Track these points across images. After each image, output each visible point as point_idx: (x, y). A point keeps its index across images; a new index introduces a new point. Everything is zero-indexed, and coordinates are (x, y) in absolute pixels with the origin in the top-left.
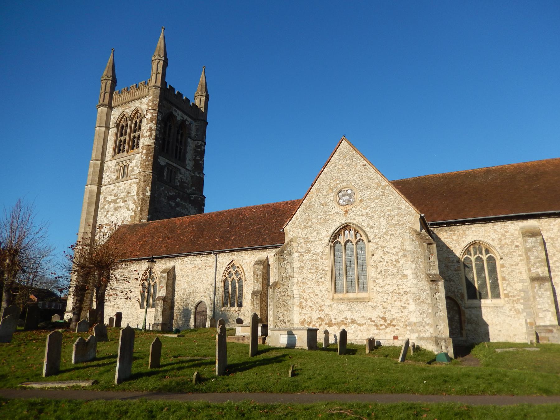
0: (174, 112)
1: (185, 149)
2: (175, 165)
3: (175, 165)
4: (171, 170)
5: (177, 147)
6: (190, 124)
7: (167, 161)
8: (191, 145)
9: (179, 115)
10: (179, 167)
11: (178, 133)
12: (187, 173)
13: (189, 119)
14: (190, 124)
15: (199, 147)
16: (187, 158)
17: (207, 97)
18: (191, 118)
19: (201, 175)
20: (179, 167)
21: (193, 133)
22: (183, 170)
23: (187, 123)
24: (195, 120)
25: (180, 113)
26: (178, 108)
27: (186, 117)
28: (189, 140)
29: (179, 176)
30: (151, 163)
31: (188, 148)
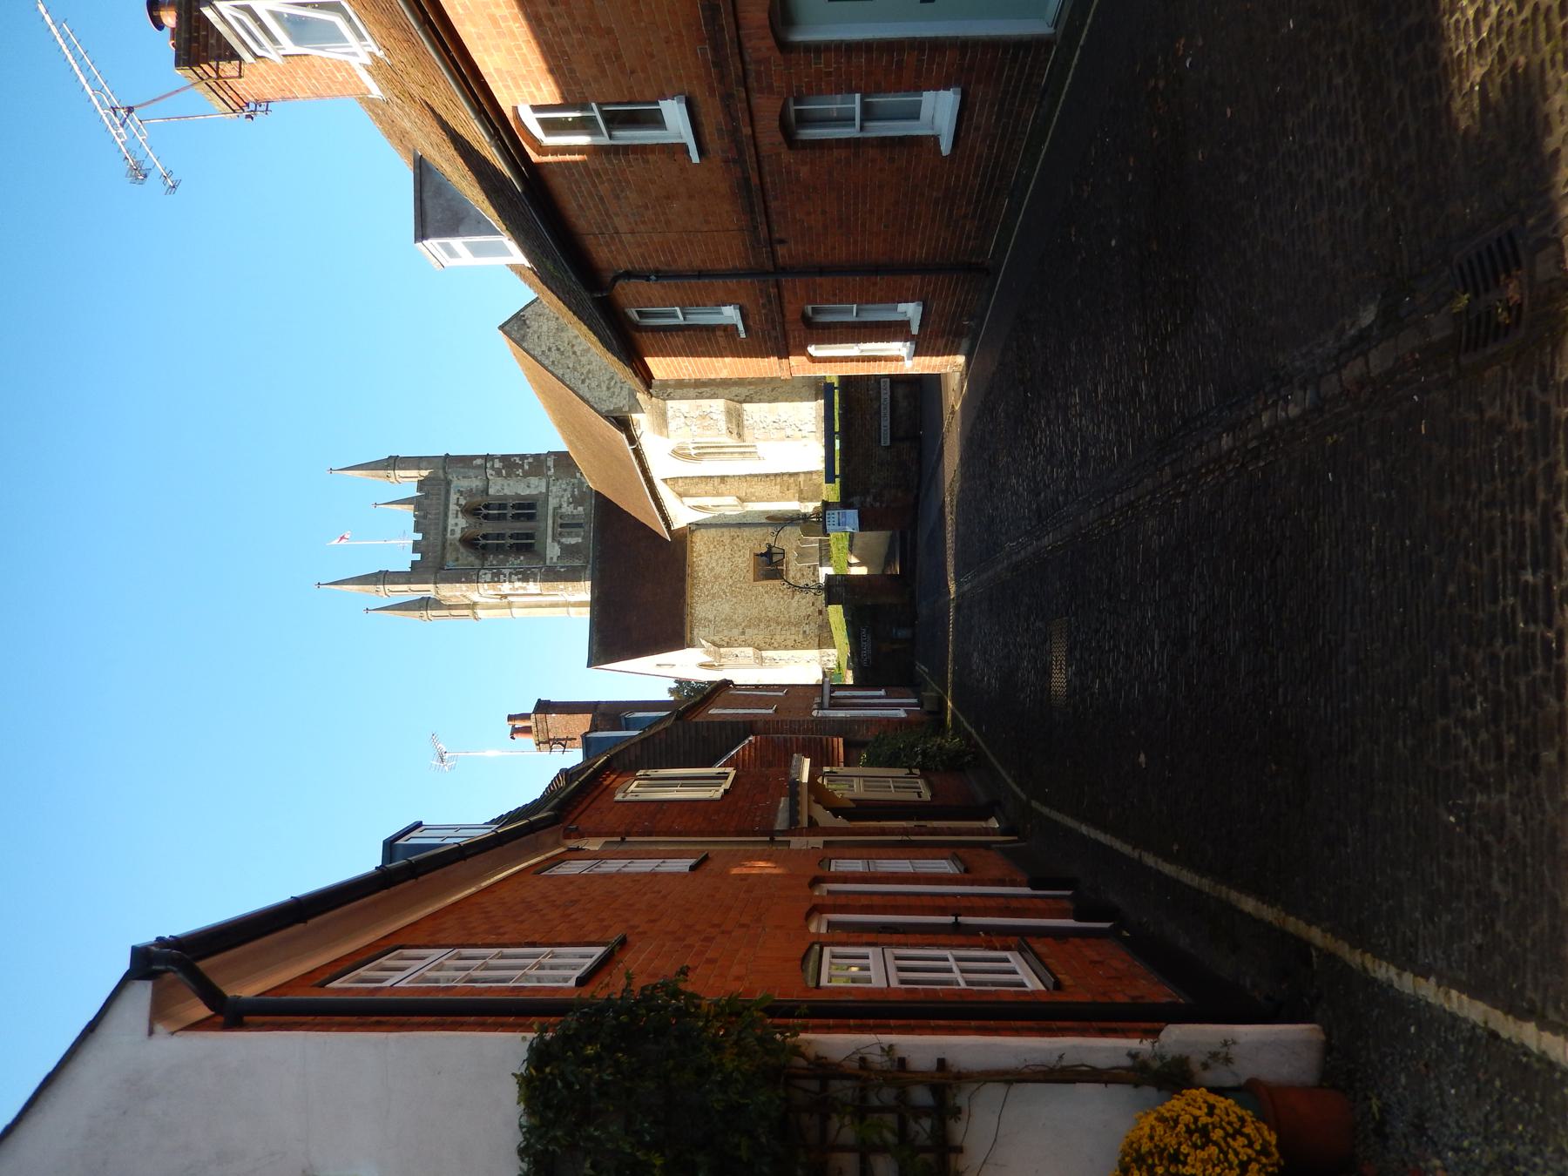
0: (458, 535)
1: (511, 497)
2: (550, 522)
3: (550, 522)
4: (562, 526)
5: (513, 516)
6: (461, 493)
7: (549, 540)
8: (501, 487)
9: (458, 524)
10: (550, 512)
11: (486, 517)
12: (554, 489)
13: (453, 497)
14: (461, 493)
15: (498, 473)
16: (527, 492)
17: (394, 463)
18: (448, 492)
19: (550, 463)
20: (550, 512)
21: (476, 483)
22: (553, 502)
23: (463, 502)
24: (449, 483)
25: (451, 521)
26: (445, 529)
27: (453, 507)
28: (491, 491)
29: (567, 509)
30: (569, 584)
31: (507, 491)
